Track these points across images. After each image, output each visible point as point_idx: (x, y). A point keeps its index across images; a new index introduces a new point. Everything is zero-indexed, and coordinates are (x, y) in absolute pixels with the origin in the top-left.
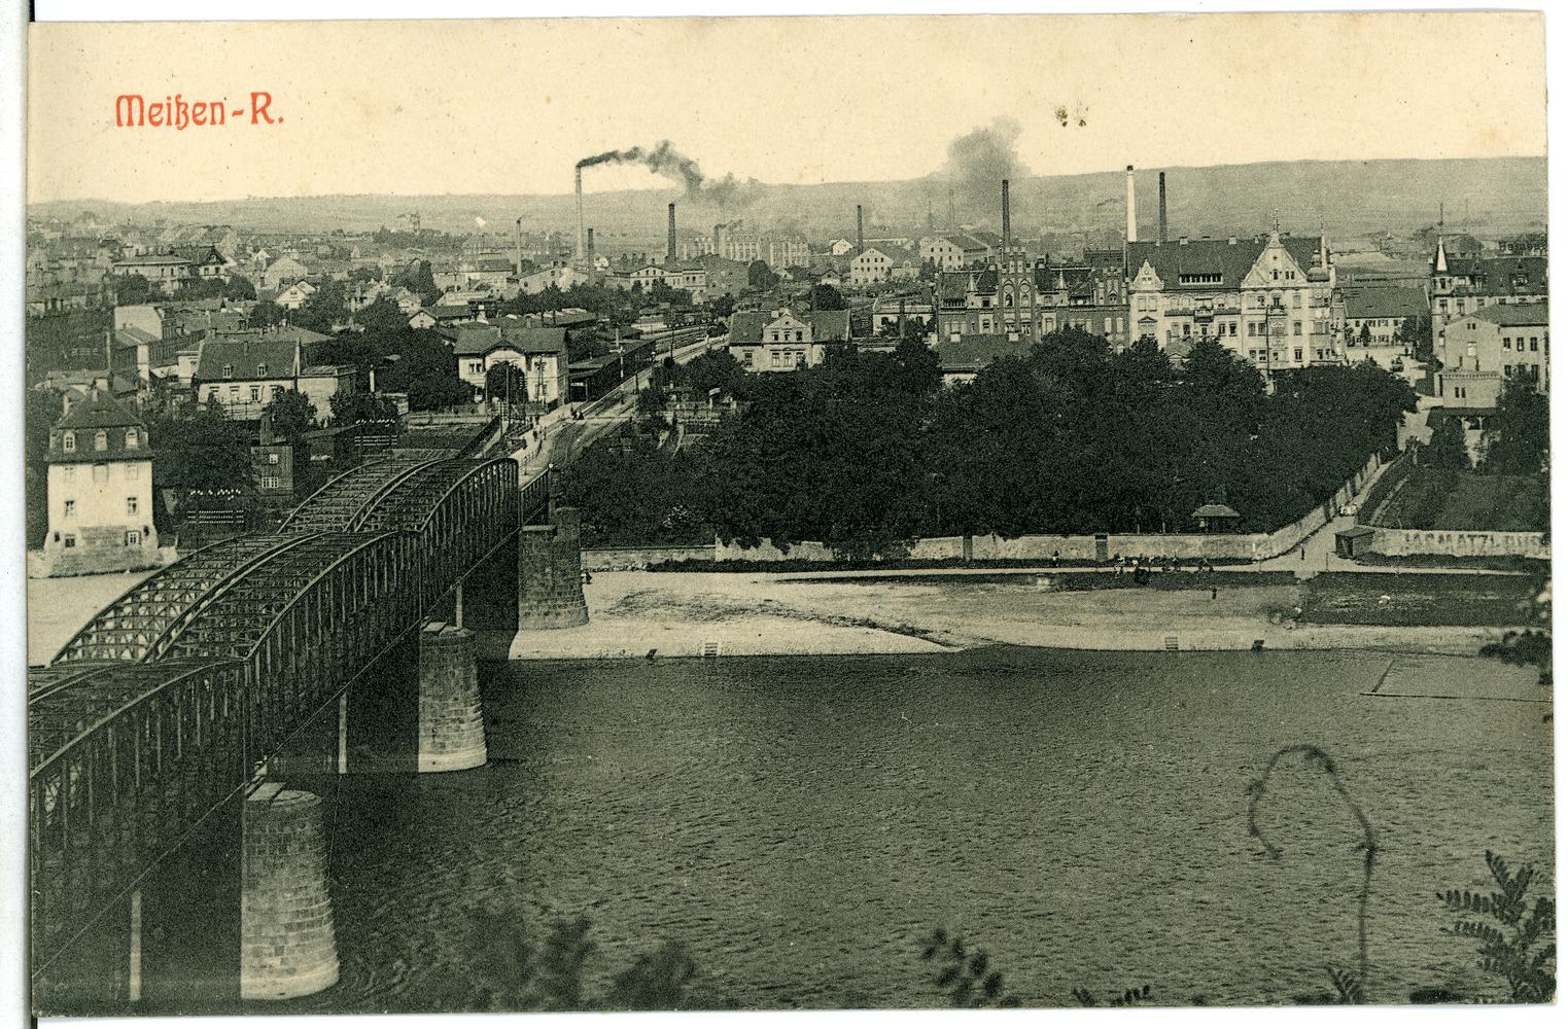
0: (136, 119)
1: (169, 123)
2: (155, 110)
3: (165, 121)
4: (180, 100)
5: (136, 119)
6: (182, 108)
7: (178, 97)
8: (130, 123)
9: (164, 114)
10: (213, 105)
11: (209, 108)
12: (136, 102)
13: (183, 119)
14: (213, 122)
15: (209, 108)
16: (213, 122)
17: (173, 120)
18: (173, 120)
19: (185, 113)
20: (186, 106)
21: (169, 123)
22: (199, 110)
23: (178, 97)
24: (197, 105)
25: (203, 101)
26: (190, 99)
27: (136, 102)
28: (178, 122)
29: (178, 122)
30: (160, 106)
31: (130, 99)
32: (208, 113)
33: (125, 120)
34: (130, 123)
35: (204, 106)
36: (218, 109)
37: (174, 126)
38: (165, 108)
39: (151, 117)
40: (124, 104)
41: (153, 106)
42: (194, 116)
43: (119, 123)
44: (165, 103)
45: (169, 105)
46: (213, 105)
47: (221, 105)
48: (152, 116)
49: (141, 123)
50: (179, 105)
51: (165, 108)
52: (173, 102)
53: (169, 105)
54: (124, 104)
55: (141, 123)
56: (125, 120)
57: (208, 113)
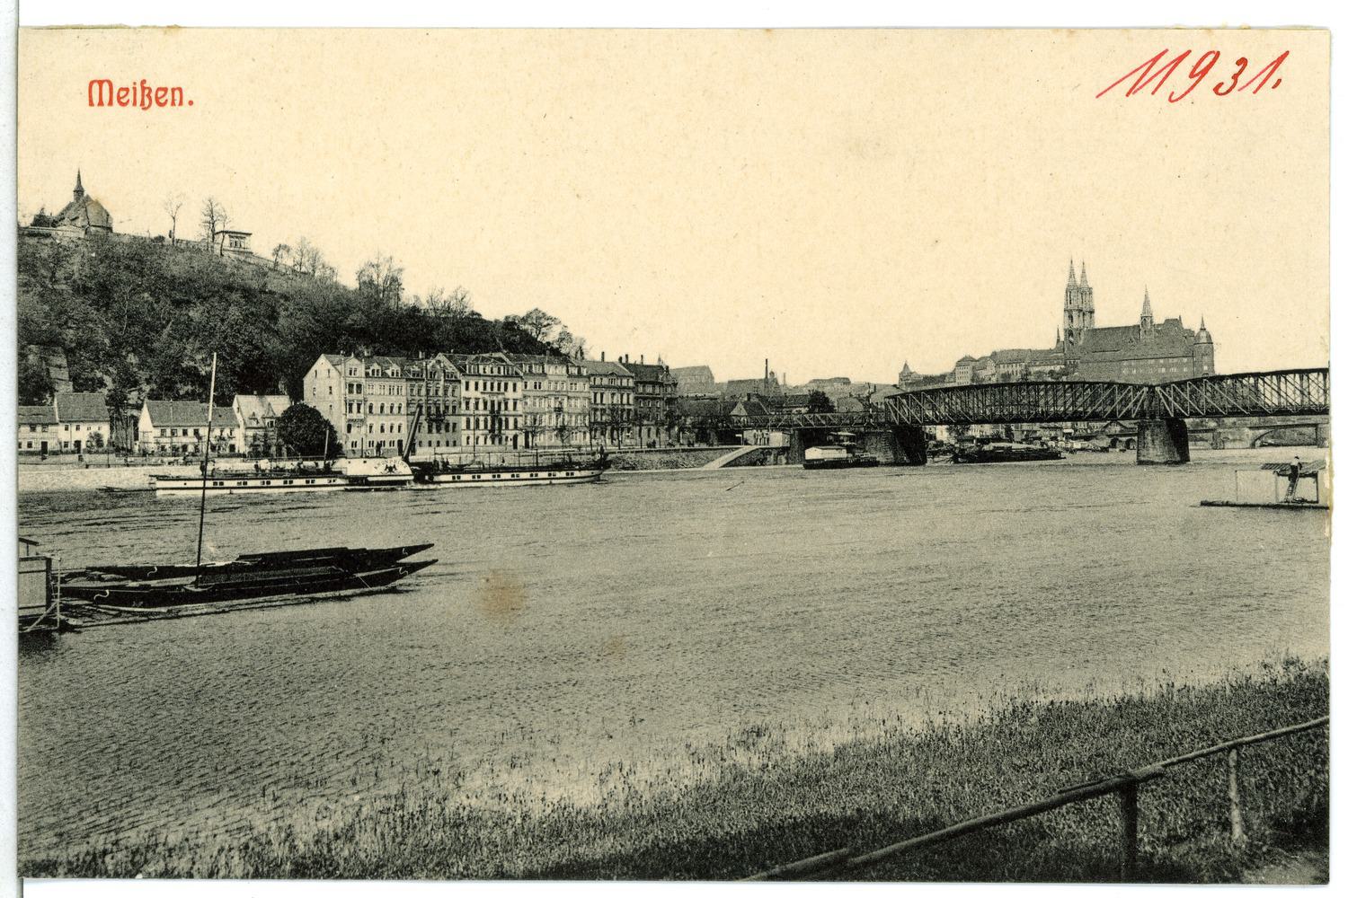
0: (106, 98)
1: (135, 104)
2: (122, 93)
5: (106, 98)
6: (147, 92)
7: (143, 82)
8: (101, 103)
9: (130, 96)
10: (173, 90)
11: (170, 92)
12: (106, 87)
14: (173, 104)
15: (170, 92)
19: (149, 96)
20: (150, 90)
21: (135, 104)
23: (143, 82)
26: (153, 84)
27: (106, 87)
28: (142, 103)
29: (142, 103)
30: (127, 90)
31: (101, 83)
32: (169, 96)
33: (96, 100)
34: (101, 103)
35: (165, 90)
36: (177, 93)
39: (119, 98)
40: (96, 87)
41: (121, 89)
43: (91, 104)
45: (135, 89)
46: (173, 90)
47: (180, 89)
48: (121, 98)
49: (110, 103)
50: (143, 89)
53: (135, 89)
54: (96, 87)
55: (110, 103)
56: (96, 100)
57: (169, 96)
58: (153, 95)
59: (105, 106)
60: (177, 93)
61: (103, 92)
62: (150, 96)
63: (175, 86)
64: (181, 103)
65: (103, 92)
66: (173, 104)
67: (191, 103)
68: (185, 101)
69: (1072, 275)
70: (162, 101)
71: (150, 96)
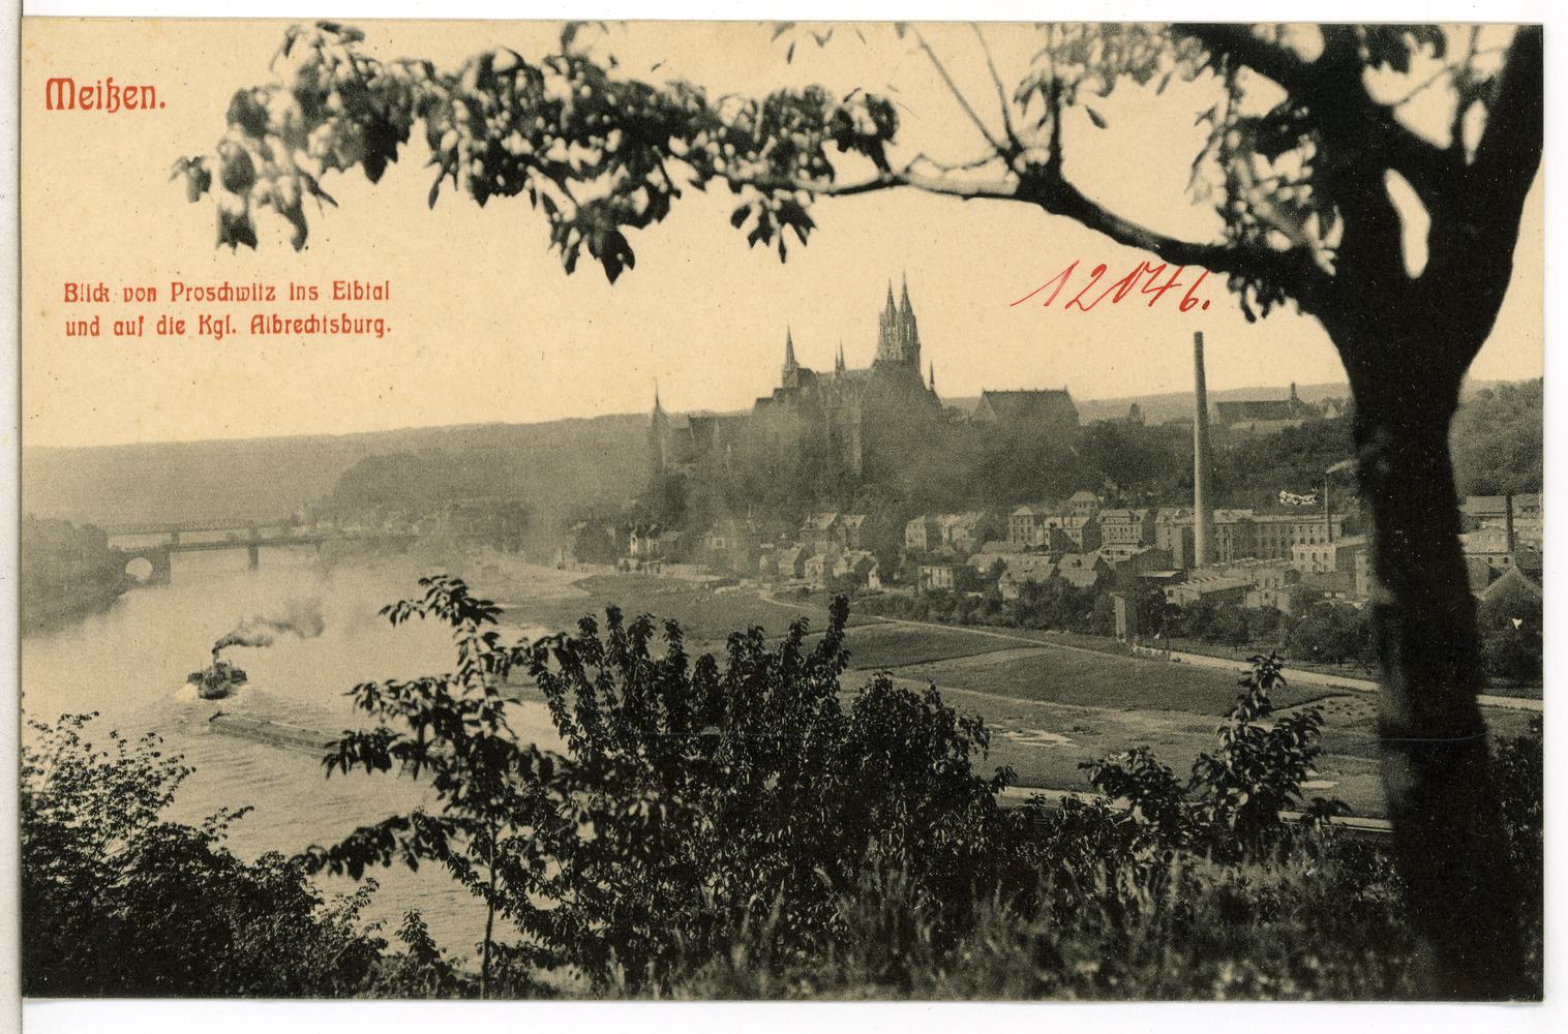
0: (66, 101)
1: (99, 106)
5: (66, 101)
6: (114, 91)
8: (60, 106)
9: (95, 97)
12: (66, 87)
13: (114, 102)
14: (144, 106)
17: (104, 102)
18: (104, 102)
19: (116, 96)
20: (118, 89)
21: (99, 106)
22: (129, 94)
23: (110, 80)
25: (133, 85)
27: (66, 87)
28: (109, 105)
29: (109, 105)
30: (91, 90)
31: (60, 82)
33: (55, 102)
34: (60, 106)
37: (104, 110)
38: (96, 92)
40: (55, 86)
41: (84, 89)
42: (126, 100)
43: (49, 106)
44: (95, 86)
46: (144, 89)
47: (152, 88)
48: (84, 98)
49: (72, 106)
50: (110, 88)
51: (96, 92)
53: (99, 89)
54: (55, 86)
55: (72, 106)
56: (55, 102)
58: (121, 96)
59: (66, 112)
63: (147, 84)
67: (163, 105)
68: (158, 103)
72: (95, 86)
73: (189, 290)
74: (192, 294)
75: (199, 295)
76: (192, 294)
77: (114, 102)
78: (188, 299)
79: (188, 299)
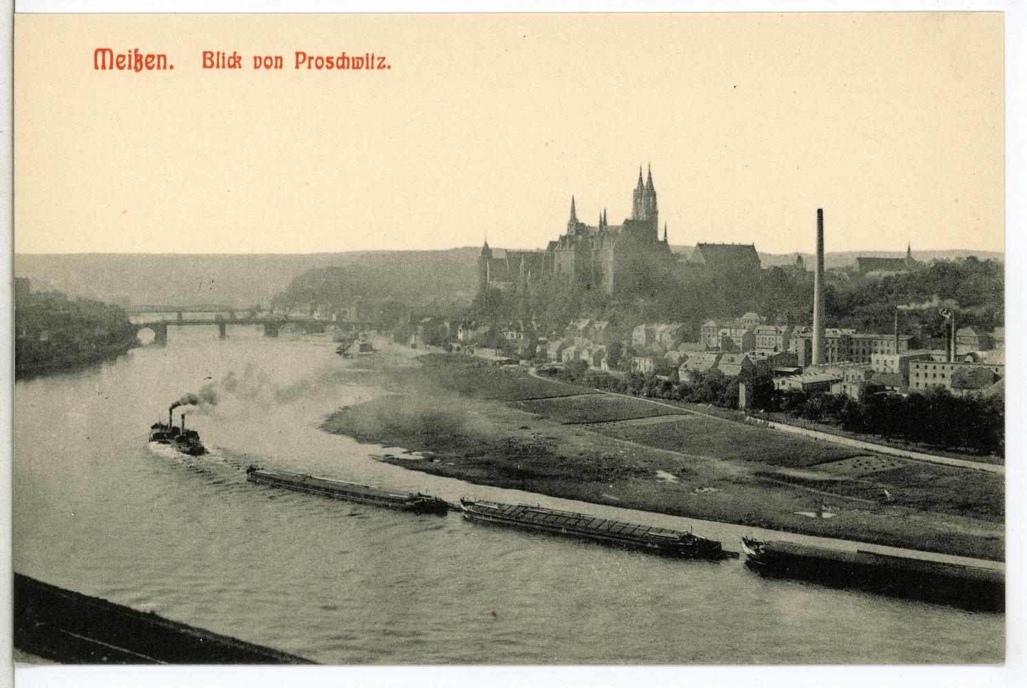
0: (108, 64)
3: (127, 67)
4: (138, 53)
5: (108, 64)
7: (136, 50)
9: (126, 62)
12: (107, 54)
13: (138, 64)
16: (159, 67)
17: (133, 65)
18: (133, 65)
23: (136, 50)
24: (149, 56)
26: (144, 52)
27: (107, 54)
30: (124, 56)
31: (104, 51)
32: (156, 61)
33: (100, 64)
34: (104, 67)
35: (153, 56)
36: (162, 60)
37: (133, 70)
40: (100, 55)
41: (119, 56)
43: (96, 67)
44: (126, 54)
45: (130, 56)
46: (159, 57)
47: (164, 56)
49: (111, 67)
50: (136, 55)
51: (127, 58)
52: (133, 54)
53: (130, 56)
54: (100, 55)
55: (111, 67)
56: (100, 64)
57: (156, 61)
58: (143, 60)
60: (162, 60)
61: (105, 58)
62: (140, 62)
63: (161, 53)
64: (165, 67)
65: (105, 58)
66: (159, 67)
67: (172, 67)
68: (168, 67)
69: (641, 180)
70: (150, 65)
71: (140, 62)
72: (126, 54)
73: (311, 58)
74: (313, 62)
75: (320, 63)
76: (313, 62)
77: (138, 64)
78: (309, 67)
79: (309, 67)
